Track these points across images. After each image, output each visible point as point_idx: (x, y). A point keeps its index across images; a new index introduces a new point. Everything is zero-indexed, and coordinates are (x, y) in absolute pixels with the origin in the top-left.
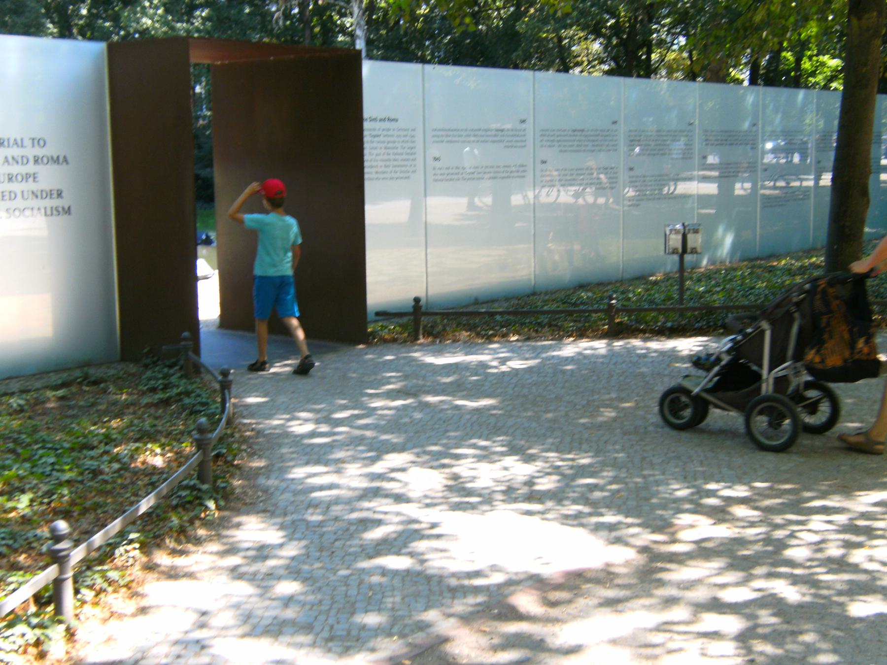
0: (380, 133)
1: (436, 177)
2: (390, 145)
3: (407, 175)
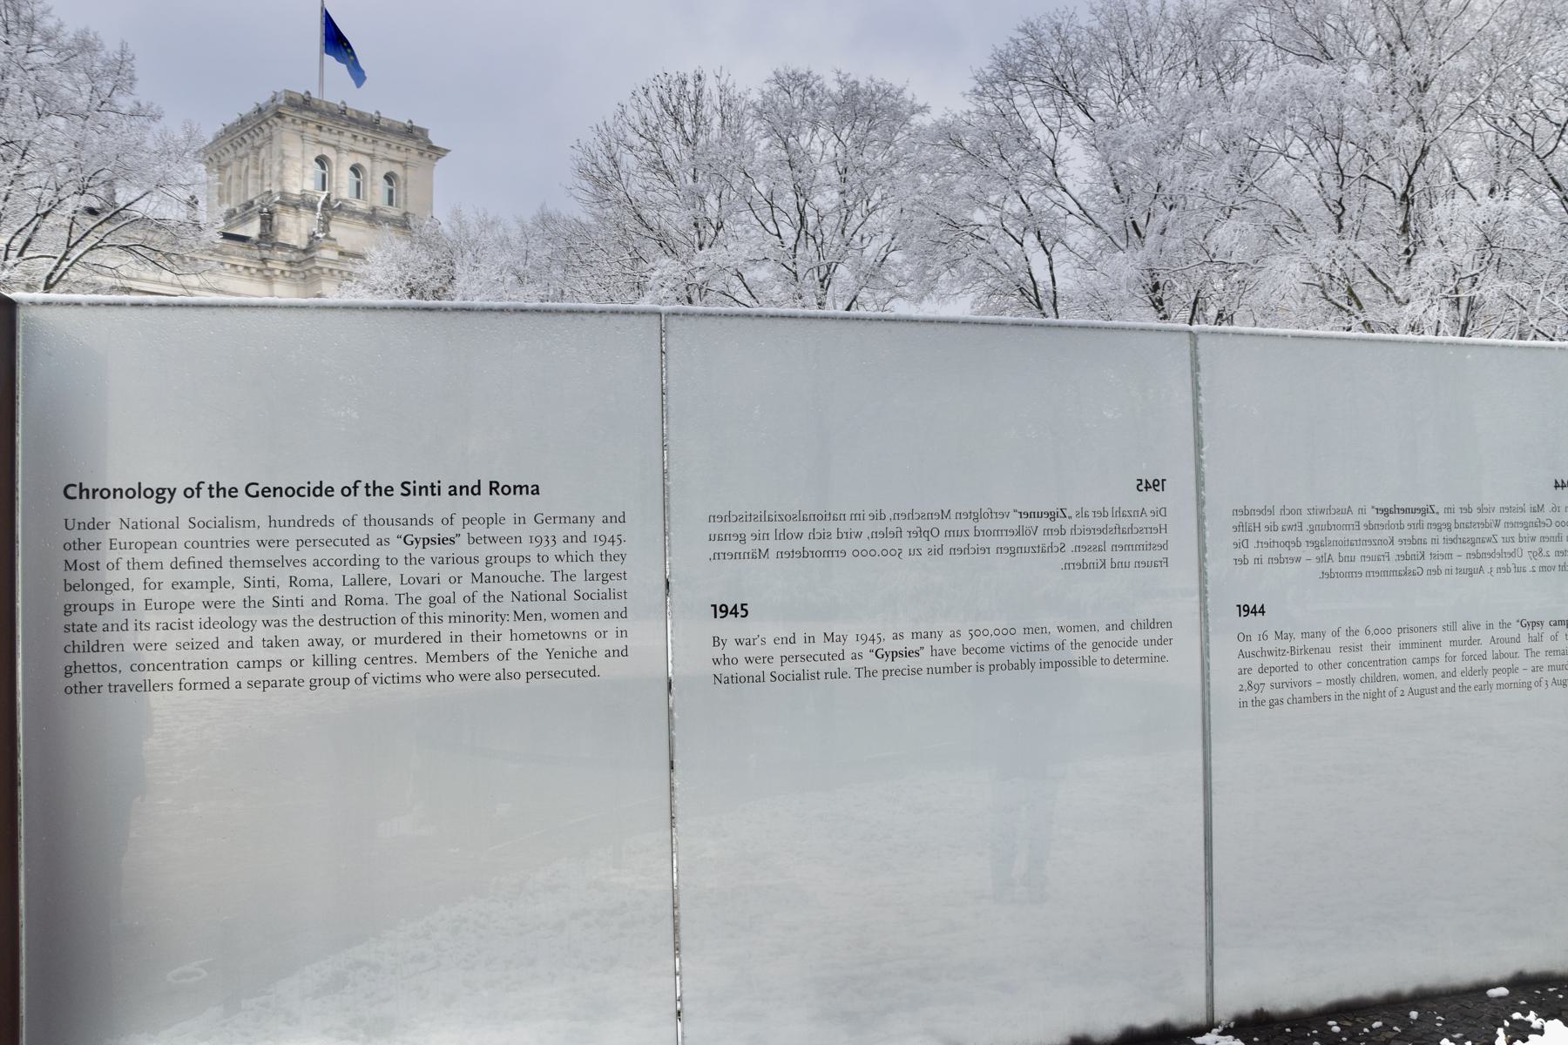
0: (447, 532)
1: (727, 670)
3: (586, 664)
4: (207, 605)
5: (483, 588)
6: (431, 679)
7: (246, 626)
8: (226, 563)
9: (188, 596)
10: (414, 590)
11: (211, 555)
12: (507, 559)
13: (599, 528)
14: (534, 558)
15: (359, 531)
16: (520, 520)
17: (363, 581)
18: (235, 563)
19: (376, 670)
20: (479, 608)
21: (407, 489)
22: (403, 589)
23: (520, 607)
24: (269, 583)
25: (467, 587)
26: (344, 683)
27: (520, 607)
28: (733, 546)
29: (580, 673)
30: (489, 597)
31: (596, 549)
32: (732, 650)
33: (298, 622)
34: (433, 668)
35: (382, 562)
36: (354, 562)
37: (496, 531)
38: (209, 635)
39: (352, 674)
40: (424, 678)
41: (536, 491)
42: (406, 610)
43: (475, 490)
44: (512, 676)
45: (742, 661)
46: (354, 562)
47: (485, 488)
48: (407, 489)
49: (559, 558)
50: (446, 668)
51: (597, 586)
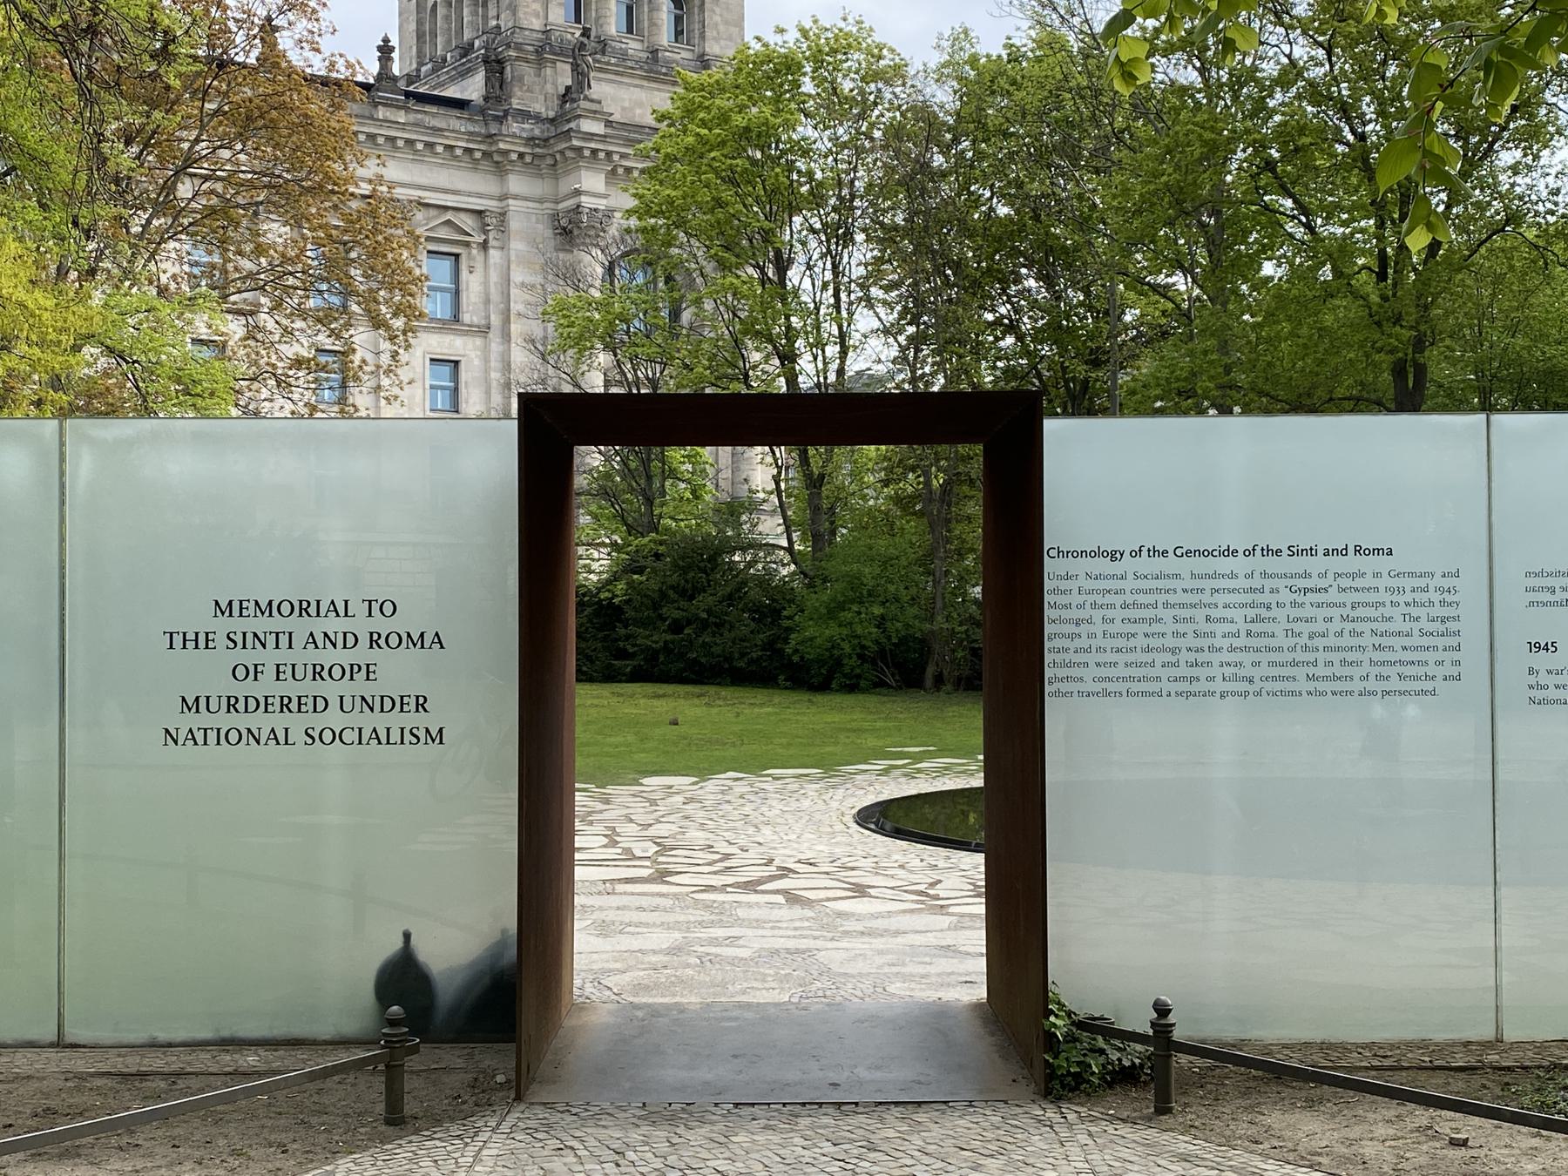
0: (1322, 583)
1: (1539, 694)
2: (1361, 612)
3: (1428, 686)
4: (1146, 635)
5: (1349, 626)
6: (1309, 693)
7: (1173, 651)
8: (1160, 605)
9: (1132, 628)
10: (1297, 627)
11: (1149, 599)
12: (1367, 604)
13: (1438, 581)
14: (1388, 604)
15: (1257, 582)
16: (1377, 575)
17: (1259, 619)
18: (1167, 605)
19: (1269, 686)
20: (1347, 641)
21: (1293, 552)
22: (1289, 626)
23: (1377, 640)
24: (1191, 620)
25: (1336, 626)
26: (1245, 694)
27: (1377, 640)
28: (1546, 597)
29: (1424, 692)
30: (1353, 633)
31: (1436, 597)
32: (1543, 679)
33: (1212, 649)
34: (1311, 686)
35: (1274, 606)
36: (1253, 605)
37: (1359, 583)
38: (1148, 658)
39: (1251, 688)
40: (1304, 693)
41: (1390, 553)
42: (1292, 641)
43: (1344, 552)
44: (1371, 693)
45: (1552, 687)
46: (1253, 605)
47: (1351, 550)
48: (1293, 552)
49: (1407, 604)
50: (1321, 686)
51: (1437, 626)
